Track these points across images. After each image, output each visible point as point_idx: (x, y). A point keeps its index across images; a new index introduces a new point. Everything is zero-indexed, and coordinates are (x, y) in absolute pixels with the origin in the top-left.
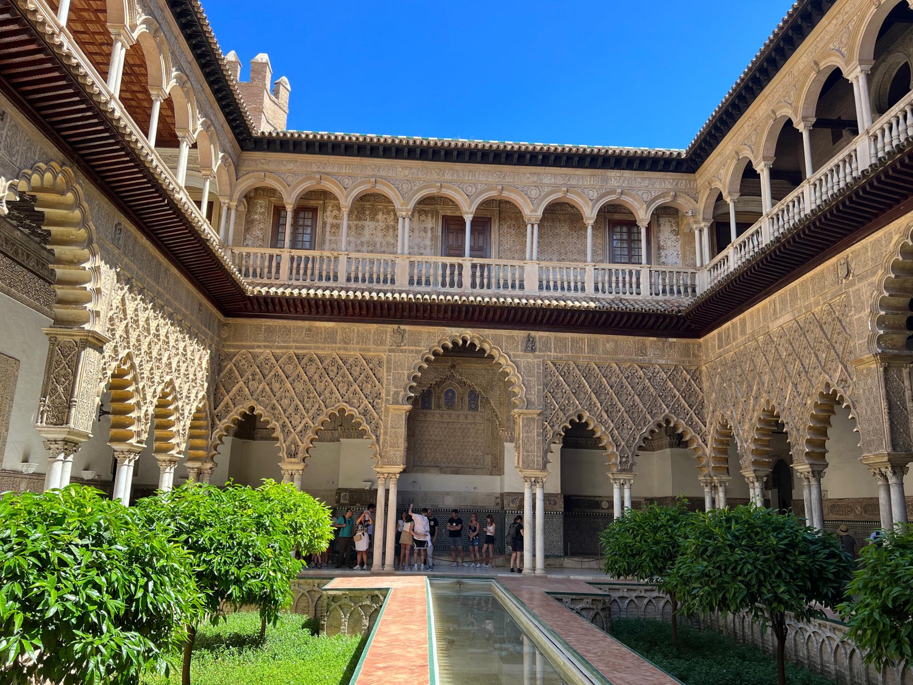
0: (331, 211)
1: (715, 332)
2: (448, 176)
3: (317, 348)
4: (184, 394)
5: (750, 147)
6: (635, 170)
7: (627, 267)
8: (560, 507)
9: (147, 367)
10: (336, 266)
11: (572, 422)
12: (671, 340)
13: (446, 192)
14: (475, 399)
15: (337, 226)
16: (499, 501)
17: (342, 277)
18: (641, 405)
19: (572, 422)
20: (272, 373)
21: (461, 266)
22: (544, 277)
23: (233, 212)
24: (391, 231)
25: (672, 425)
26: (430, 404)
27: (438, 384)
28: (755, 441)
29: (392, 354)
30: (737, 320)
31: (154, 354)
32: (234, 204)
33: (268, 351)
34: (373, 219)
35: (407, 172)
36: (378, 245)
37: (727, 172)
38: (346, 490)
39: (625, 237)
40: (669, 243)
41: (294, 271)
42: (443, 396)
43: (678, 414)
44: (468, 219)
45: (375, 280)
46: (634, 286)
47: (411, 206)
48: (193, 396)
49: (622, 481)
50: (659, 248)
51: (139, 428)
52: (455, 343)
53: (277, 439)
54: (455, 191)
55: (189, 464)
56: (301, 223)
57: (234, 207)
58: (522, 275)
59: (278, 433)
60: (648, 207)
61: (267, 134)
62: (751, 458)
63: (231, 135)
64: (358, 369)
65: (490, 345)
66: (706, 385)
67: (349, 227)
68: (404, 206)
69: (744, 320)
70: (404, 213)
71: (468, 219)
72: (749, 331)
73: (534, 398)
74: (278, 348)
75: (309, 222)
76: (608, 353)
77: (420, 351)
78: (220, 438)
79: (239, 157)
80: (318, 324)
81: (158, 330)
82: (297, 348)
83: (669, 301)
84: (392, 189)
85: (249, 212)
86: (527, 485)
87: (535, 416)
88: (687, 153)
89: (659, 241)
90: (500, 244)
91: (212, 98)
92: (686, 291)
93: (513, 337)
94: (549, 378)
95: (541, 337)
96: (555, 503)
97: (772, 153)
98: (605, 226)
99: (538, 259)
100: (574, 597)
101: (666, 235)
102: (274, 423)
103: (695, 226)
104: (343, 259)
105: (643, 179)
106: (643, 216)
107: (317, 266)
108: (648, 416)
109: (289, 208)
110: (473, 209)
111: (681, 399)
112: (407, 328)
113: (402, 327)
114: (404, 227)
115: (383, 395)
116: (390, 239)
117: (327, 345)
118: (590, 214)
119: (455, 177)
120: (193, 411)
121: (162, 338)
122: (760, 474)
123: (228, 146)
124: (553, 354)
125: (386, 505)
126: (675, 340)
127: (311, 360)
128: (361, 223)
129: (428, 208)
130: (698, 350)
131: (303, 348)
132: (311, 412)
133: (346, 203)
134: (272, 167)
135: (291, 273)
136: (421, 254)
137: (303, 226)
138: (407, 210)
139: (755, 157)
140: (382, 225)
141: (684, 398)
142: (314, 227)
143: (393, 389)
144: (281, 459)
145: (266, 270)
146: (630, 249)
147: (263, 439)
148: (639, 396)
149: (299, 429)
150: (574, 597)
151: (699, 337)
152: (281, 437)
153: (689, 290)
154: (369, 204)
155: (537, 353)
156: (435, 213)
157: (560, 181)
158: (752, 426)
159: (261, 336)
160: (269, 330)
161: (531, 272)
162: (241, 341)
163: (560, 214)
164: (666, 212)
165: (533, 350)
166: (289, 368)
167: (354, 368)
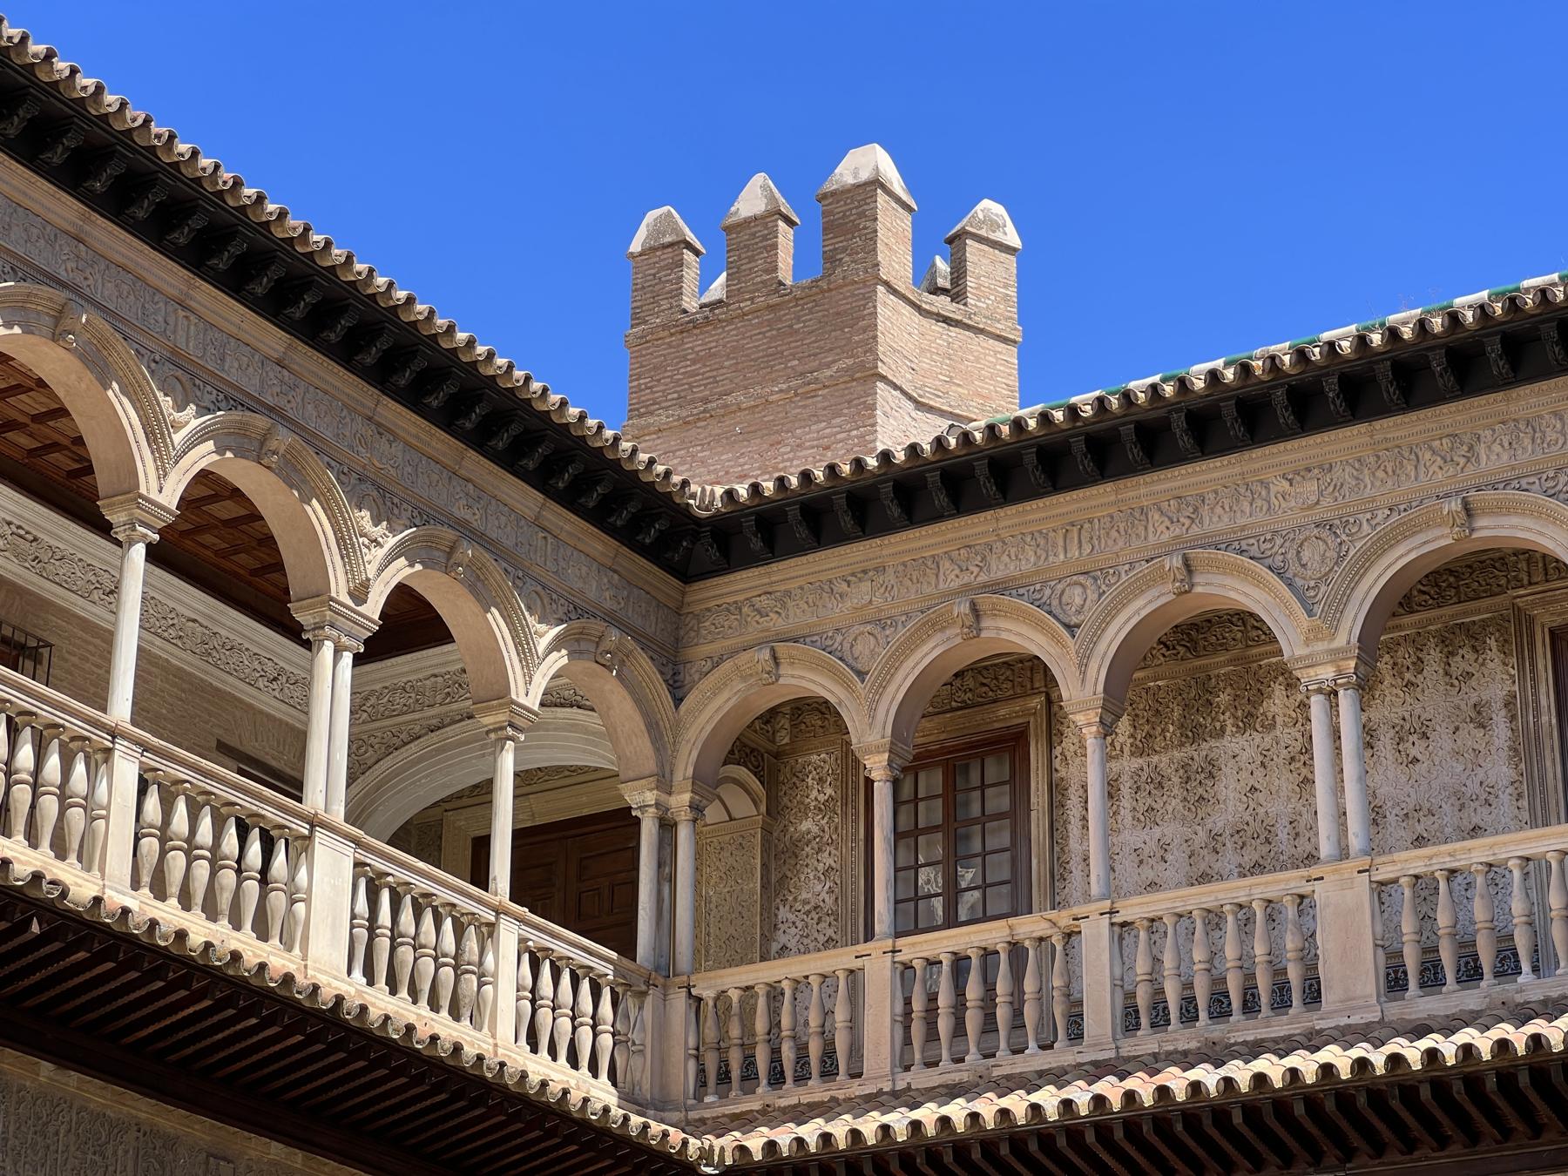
2: (1493, 458)
17: (1099, 1018)
32: (681, 801)
34: (1248, 722)
35: (1310, 488)
36: (1283, 834)
41: (917, 1030)
45: (1236, 1004)
54: (1537, 513)
57: (683, 817)
63: (598, 544)
68: (1315, 644)
75: (999, 800)
84: (1259, 582)
85: (775, 810)
91: (440, 442)
109: (877, 766)
114: (1334, 728)
119: (1527, 453)
123: (596, 589)
128: (1197, 753)
129: (1478, 612)
134: (797, 617)
135: (907, 1041)
136: (1475, 831)
138: (1336, 655)
142: (1018, 813)
154: (1201, 666)
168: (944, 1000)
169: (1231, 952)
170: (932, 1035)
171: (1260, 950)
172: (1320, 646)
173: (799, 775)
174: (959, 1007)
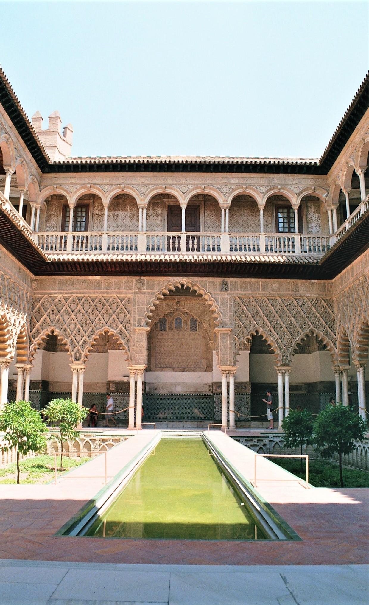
1: (339, 275)
3: (90, 293)
5: (353, 160)
6: (289, 173)
7: (286, 235)
8: (249, 390)
10: (101, 241)
11: (252, 336)
12: (313, 281)
13: (168, 191)
14: (195, 324)
15: (102, 215)
16: (211, 388)
17: (105, 247)
18: (295, 323)
19: (252, 336)
21: (179, 237)
22: (233, 242)
23: (38, 211)
24: (135, 217)
25: (315, 335)
26: (165, 328)
27: (171, 314)
28: (360, 342)
29: (137, 295)
30: (349, 267)
33: (61, 296)
34: (123, 210)
37: (343, 174)
38: (113, 382)
39: (286, 215)
40: (314, 219)
41: (75, 245)
42: (174, 322)
43: (319, 328)
44: (184, 207)
46: (291, 247)
47: (147, 200)
49: (283, 371)
50: (307, 222)
52: (177, 288)
53: (67, 351)
54: (175, 190)
55: (18, 365)
56: (79, 214)
58: (219, 242)
59: (69, 346)
60: (298, 196)
61: (57, 162)
62: (357, 352)
63: (36, 165)
64: (115, 305)
65: (199, 287)
66: (336, 309)
67: (109, 216)
69: (353, 266)
70: (143, 206)
71: (184, 207)
72: (355, 274)
73: (227, 321)
74: (66, 293)
75: (84, 214)
76: (274, 290)
77: (154, 293)
78: (35, 350)
79: (41, 177)
80: (90, 278)
82: (77, 293)
83: (313, 257)
85: (48, 210)
86: (224, 375)
87: (228, 332)
88: (320, 162)
89: (307, 218)
90: (206, 223)
91: (24, 145)
92: (323, 250)
93: (213, 282)
94: (238, 308)
95: (231, 282)
96: (246, 388)
97: (365, 164)
98: (273, 210)
99: (230, 231)
100: (246, 439)
101: (312, 214)
103: (328, 208)
104: (105, 236)
105: (294, 179)
106: (295, 202)
107: (89, 241)
108: (300, 330)
109: (72, 207)
110: (187, 200)
111: (321, 318)
112: (145, 278)
113: (142, 278)
114: (143, 214)
115: (131, 321)
116: (134, 221)
117: (95, 291)
118: (262, 202)
119: (174, 182)
122: (361, 362)
123: (34, 172)
124: (239, 292)
125: (136, 391)
126: (316, 281)
127: (87, 301)
128: (116, 213)
130: (331, 287)
131: (80, 293)
132: (88, 332)
133: (106, 201)
135: (73, 247)
137: (81, 217)
139: (356, 167)
140: (129, 213)
141: (322, 318)
143: (138, 318)
145: (58, 246)
146: (289, 223)
147: (61, 351)
148: (294, 317)
149: (81, 343)
150: (246, 439)
151: (332, 279)
152: (71, 349)
153: (326, 249)
155: (229, 292)
156: (163, 205)
157: (241, 182)
158: (358, 333)
159: (56, 287)
160: (61, 282)
161: (225, 241)
162: (44, 290)
163: (243, 203)
164: (310, 201)
165: (226, 290)
166: (73, 306)
167: (113, 305)
168: (80, 242)
169: (125, 242)
170: (77, 246)
171: (129, 242)
172: (143, 202)
173: (52, 205)
174: (82, 243)
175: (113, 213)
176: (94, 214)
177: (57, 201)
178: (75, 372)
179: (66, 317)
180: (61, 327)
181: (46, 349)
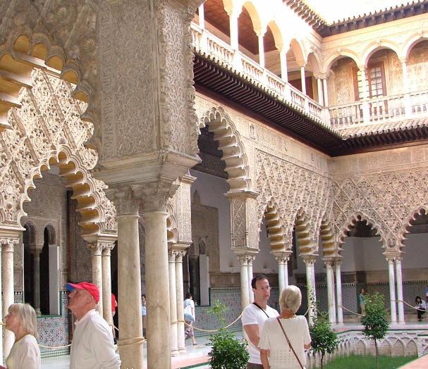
0: (394, 62)
4: (312, 215)
9: (284, 203)
15: (401, 72)
20: (369, 191)
23: (325, 82)
31: (288, 195)
32: (324, 77)
48: (318, 215)
51: (286, 241)
59: (380, 231)
80: (395, 150)
81: (286, 179)
102: (376, 225)
120: (320, 225)
121: (290, 183)
133: (402, 53)
135: (371, 114)
142: (383, 77)
144: (384, 250)
149: (394, 227)
152: (383, 235)
175: (414, 66)
176: (391, 73)
177: (343, 64)
178: (391, 262)
179: (373, 200)
180: (369, 211)
181: (356, 235)
